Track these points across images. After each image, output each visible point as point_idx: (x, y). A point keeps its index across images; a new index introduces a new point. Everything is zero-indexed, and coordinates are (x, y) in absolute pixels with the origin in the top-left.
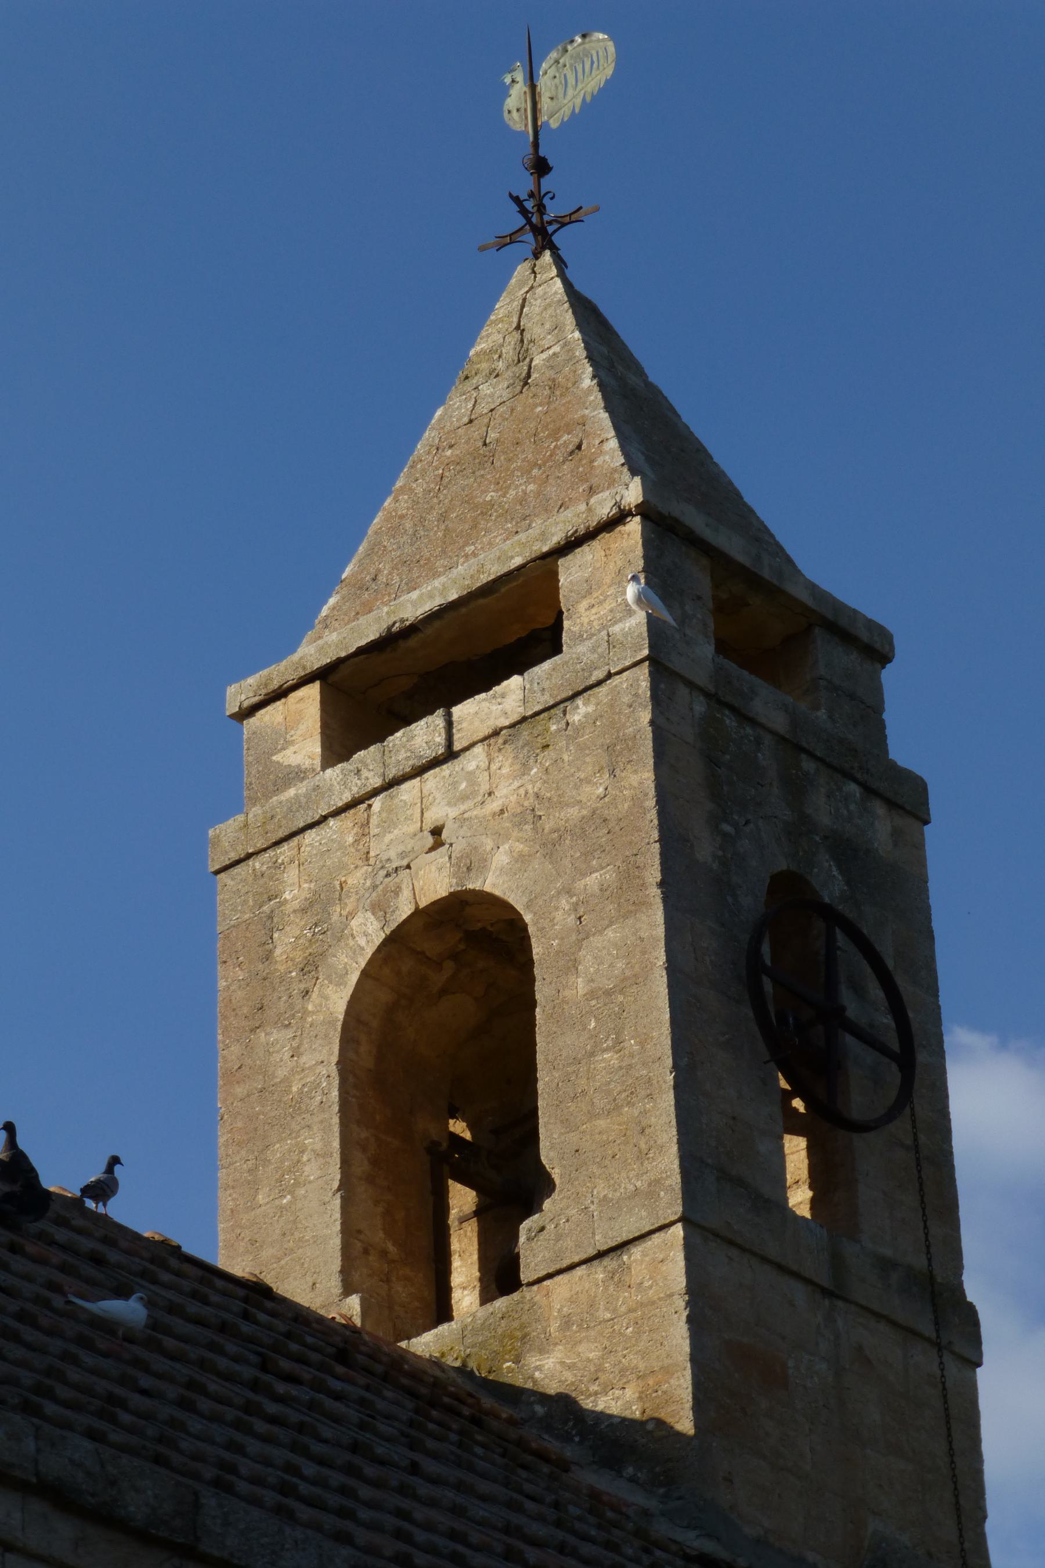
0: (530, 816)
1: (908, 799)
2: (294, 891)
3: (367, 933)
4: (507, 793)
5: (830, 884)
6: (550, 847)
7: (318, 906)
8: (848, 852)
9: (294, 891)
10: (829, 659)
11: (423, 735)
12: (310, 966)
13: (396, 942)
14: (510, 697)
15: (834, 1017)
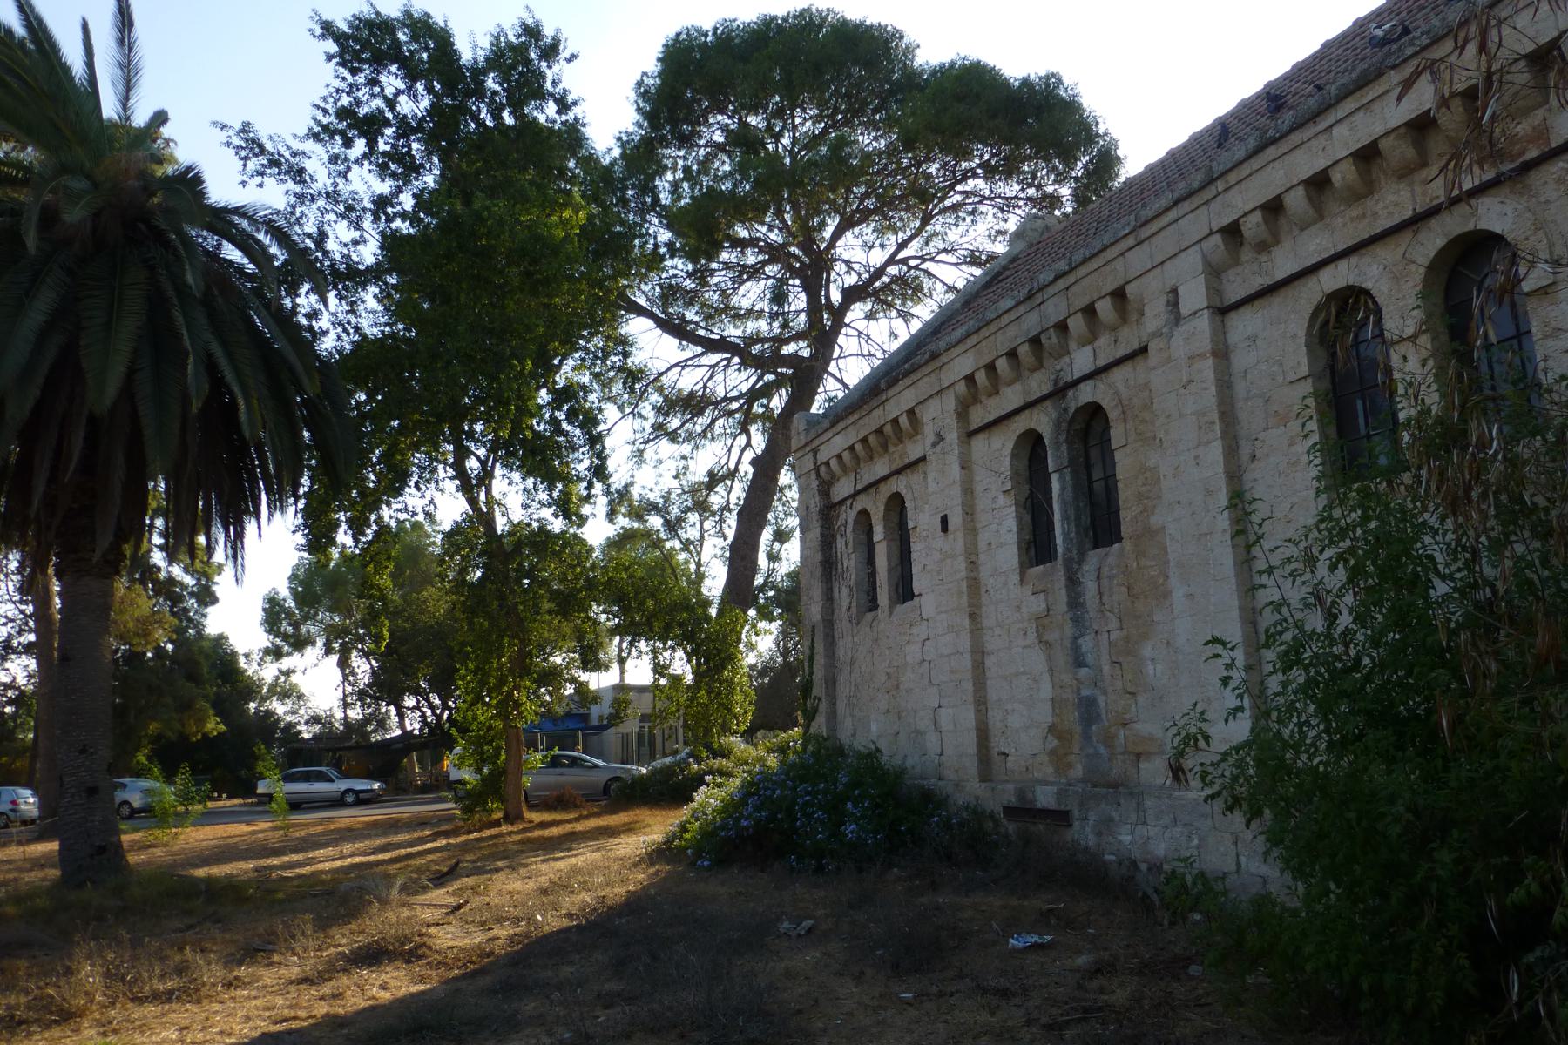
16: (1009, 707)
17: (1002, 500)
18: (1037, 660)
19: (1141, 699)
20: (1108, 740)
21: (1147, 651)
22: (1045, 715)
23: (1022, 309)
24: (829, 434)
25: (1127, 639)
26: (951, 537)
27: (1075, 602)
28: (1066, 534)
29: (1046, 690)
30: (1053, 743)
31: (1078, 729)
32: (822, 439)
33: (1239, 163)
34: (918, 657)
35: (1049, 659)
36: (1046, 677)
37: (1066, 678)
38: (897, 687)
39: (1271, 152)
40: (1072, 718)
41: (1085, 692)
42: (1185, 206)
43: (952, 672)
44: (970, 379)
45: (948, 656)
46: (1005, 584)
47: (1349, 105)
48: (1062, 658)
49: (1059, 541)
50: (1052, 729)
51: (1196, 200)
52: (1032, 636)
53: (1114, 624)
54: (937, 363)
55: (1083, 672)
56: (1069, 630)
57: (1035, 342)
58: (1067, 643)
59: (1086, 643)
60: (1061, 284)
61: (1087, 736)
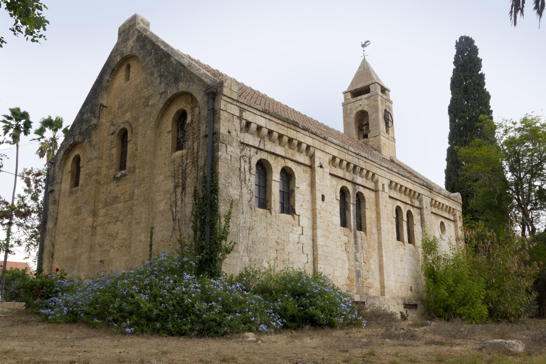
0: (367, 105)
1: (391, 102)
2: (349, 108)
3: (355, 112)
4: (366, 103)
5: (388, 110)
6: (370, 107)
7: (351, 109)
8: (388, 107)
9: (349, 108)
10: (387, 92)
11: (359, 98)
12: (350, 114)
13: (357, 112)
14: (366, 95)
15: (389, 120)
16: (335, 268)
17: (335, 201)
18: (345, 256)
19: (370, 273)
20: (363, 283)
21: (371, 262)
22: (346, 273)
23: (354, 155)
24: (259, 113)
25: (367, 257)
26: (325, 204)
27: (356, 243)
28: (354, 223)
29: (347, 266)
30: (349, 282)
31: (355, 279)
32: (250, 109)
33: (332, 143)
34: (297, 240)
35: (348, 256)
36: (347, 261)
37: (353, 263)
38: (283, 249)
39: (398, 175)
40: (354, 275)
41: (358, 269)
42: (387, 170)
43: (324, 252)
44: (334, 158)
45: (323, 246)
46: (335, 228)
47: (406, 179)
48: (352, 258)
49: (352, 223)
50: (348, 278)
51: (389, 171)
52: (344, 248)
53: (365, 252)
54: (325, 141)
55: (357, 263)
56: (354, 249)
57: (355, 166)
58: (354, 253)
59: (358, 255)
60: (364, 159)
61: (357, 281)
